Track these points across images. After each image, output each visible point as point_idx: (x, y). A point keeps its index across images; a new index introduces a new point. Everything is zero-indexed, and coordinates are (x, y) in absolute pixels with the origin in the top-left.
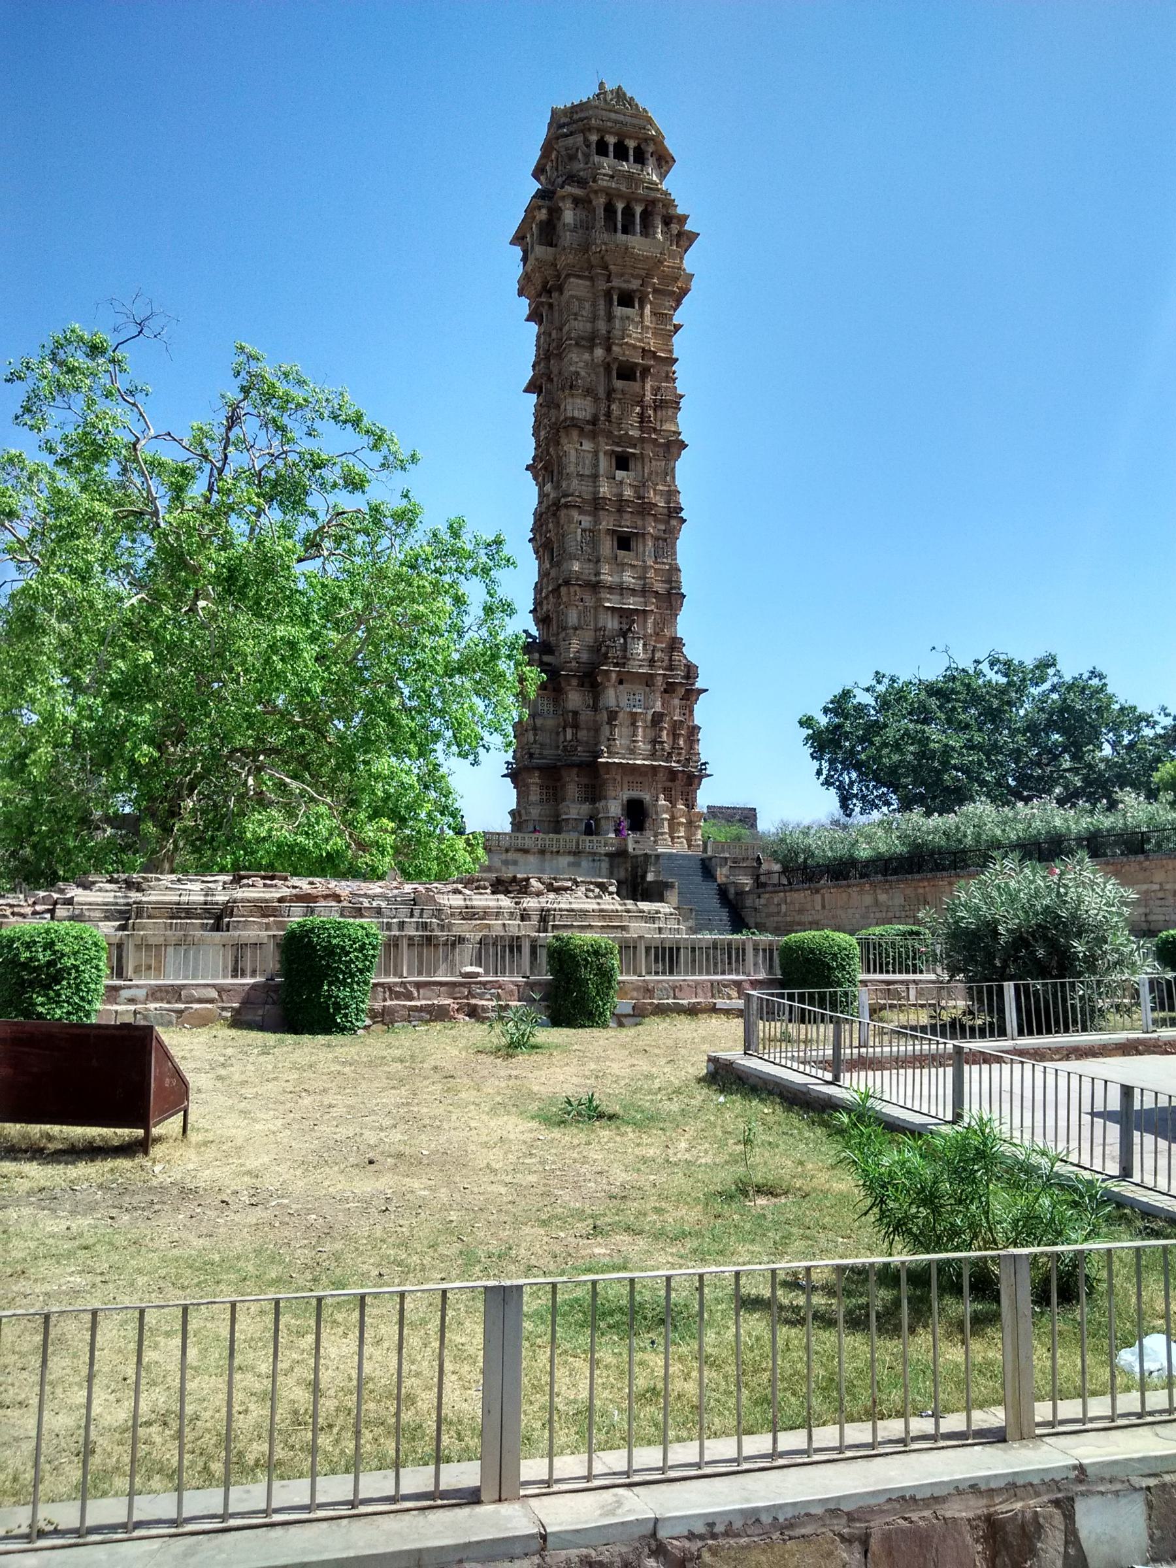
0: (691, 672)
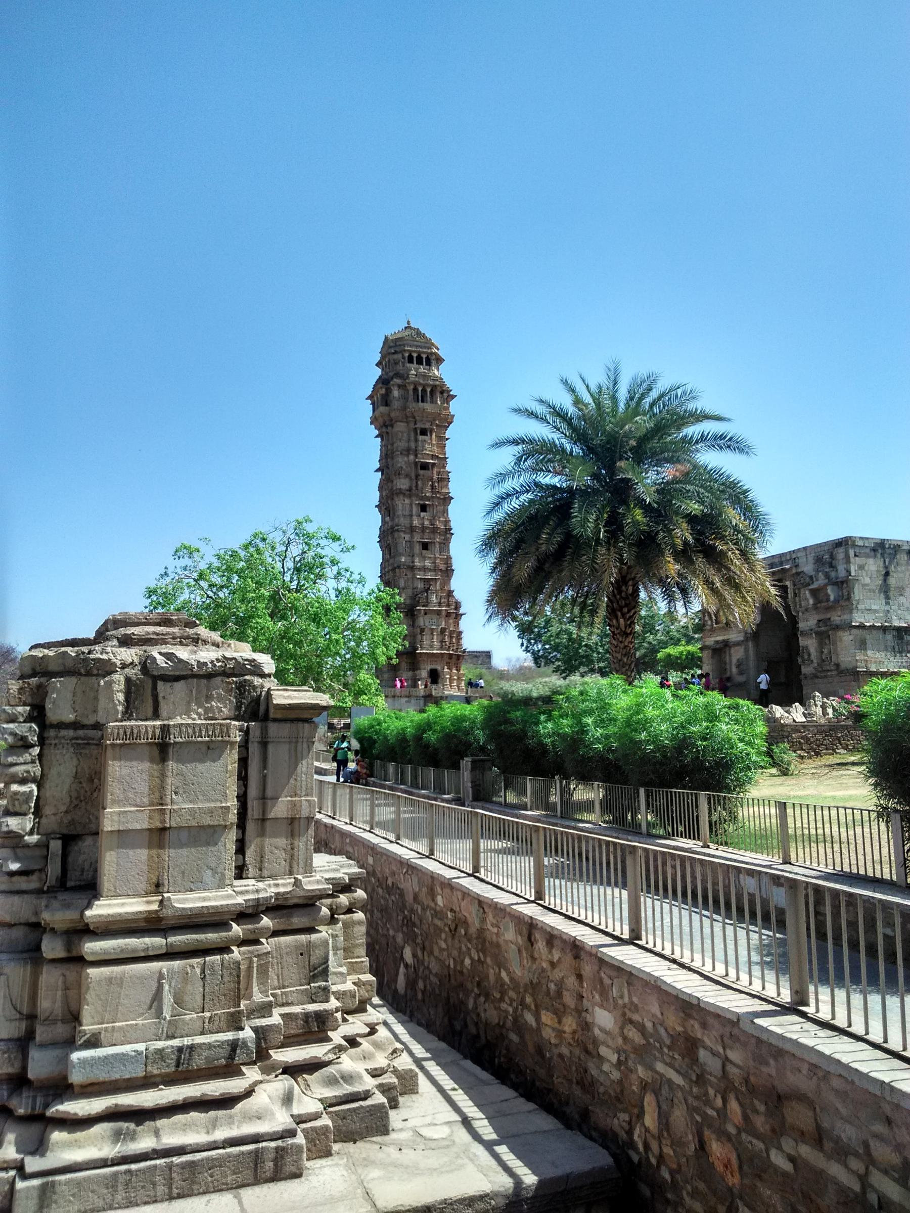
0: (458, 605)
